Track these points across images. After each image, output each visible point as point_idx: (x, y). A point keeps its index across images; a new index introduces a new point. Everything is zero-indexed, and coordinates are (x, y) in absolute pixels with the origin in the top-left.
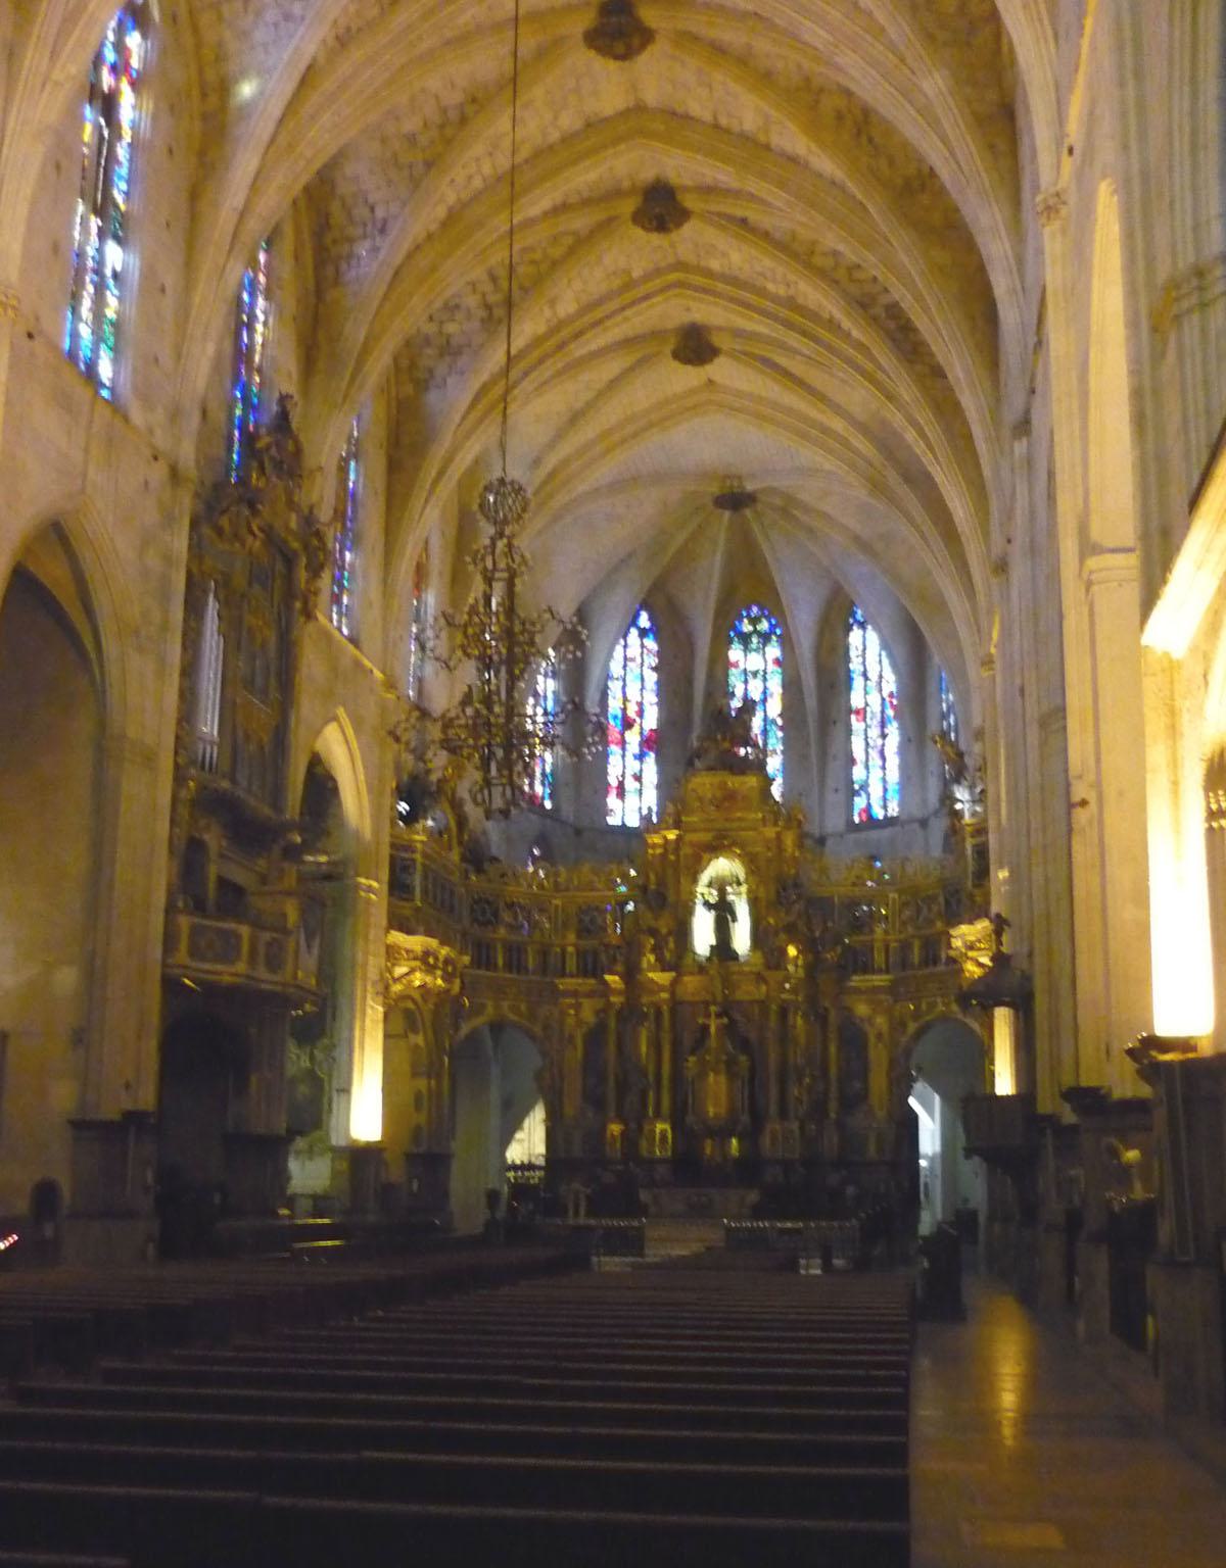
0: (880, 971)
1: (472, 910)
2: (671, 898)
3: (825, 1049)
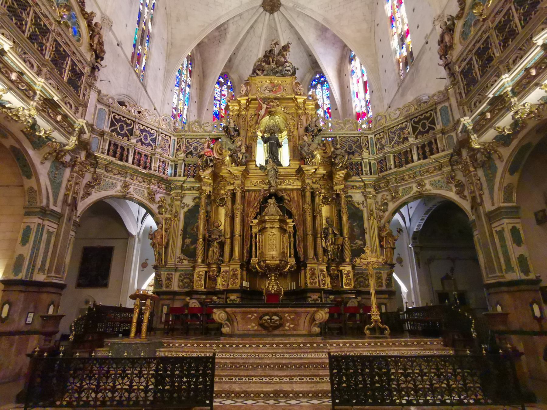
0: (367, 174)
1: (112, 124)
2: (242, 133)
3: (340, 218)
